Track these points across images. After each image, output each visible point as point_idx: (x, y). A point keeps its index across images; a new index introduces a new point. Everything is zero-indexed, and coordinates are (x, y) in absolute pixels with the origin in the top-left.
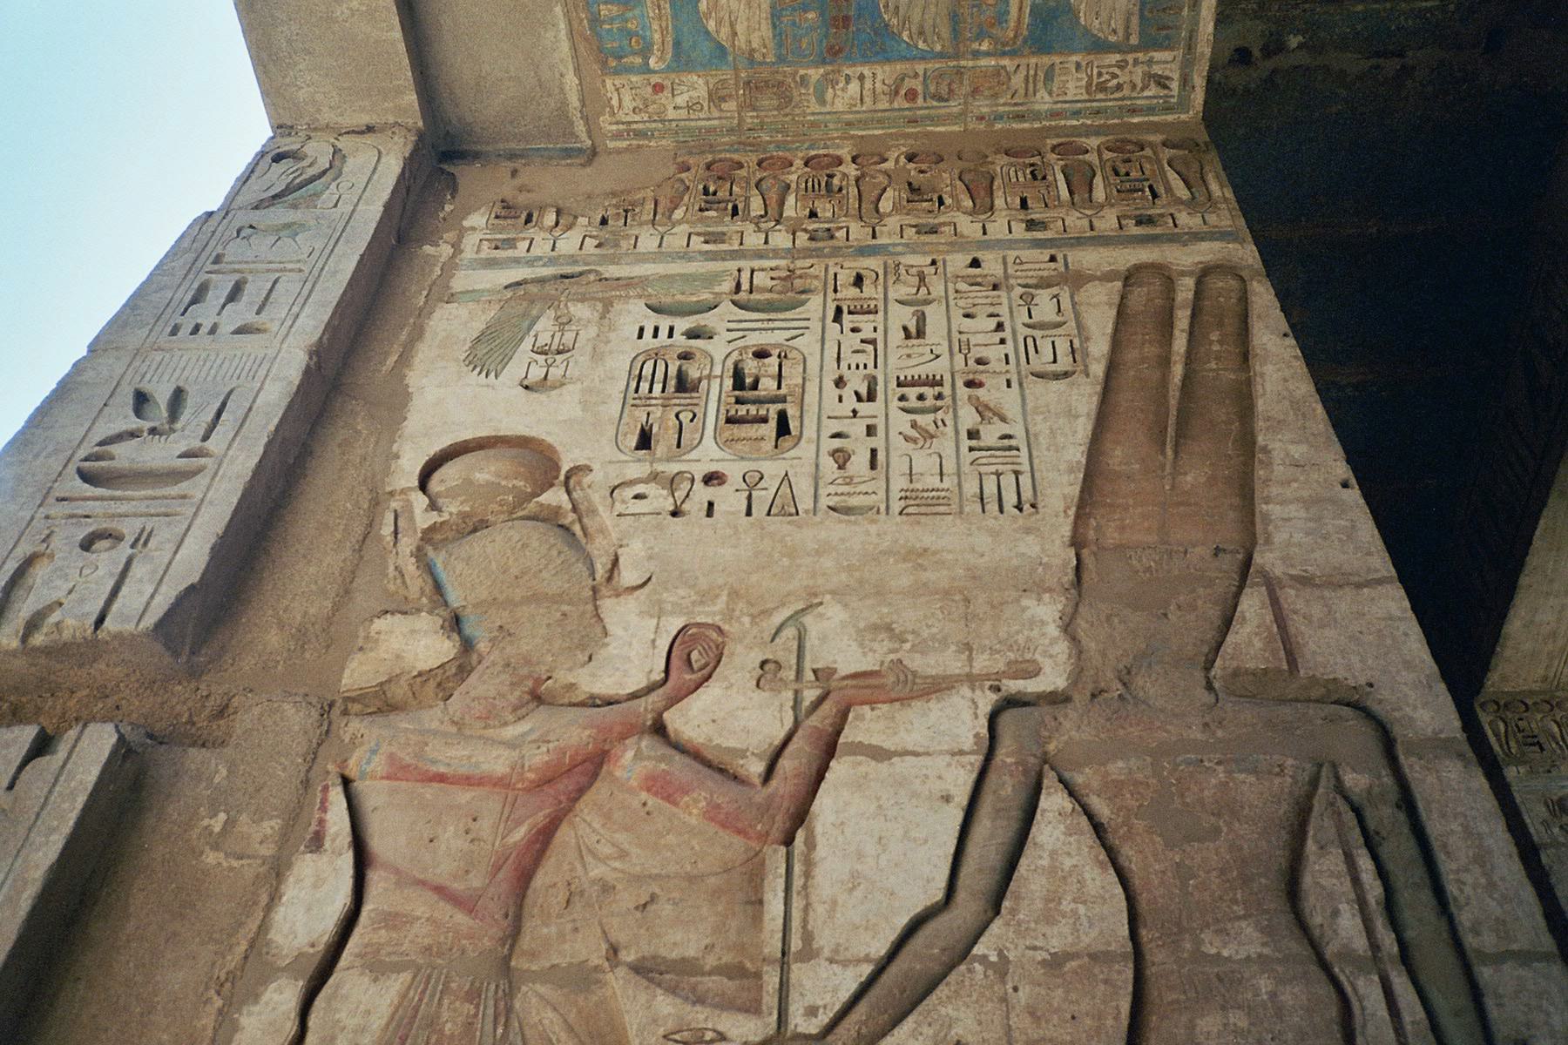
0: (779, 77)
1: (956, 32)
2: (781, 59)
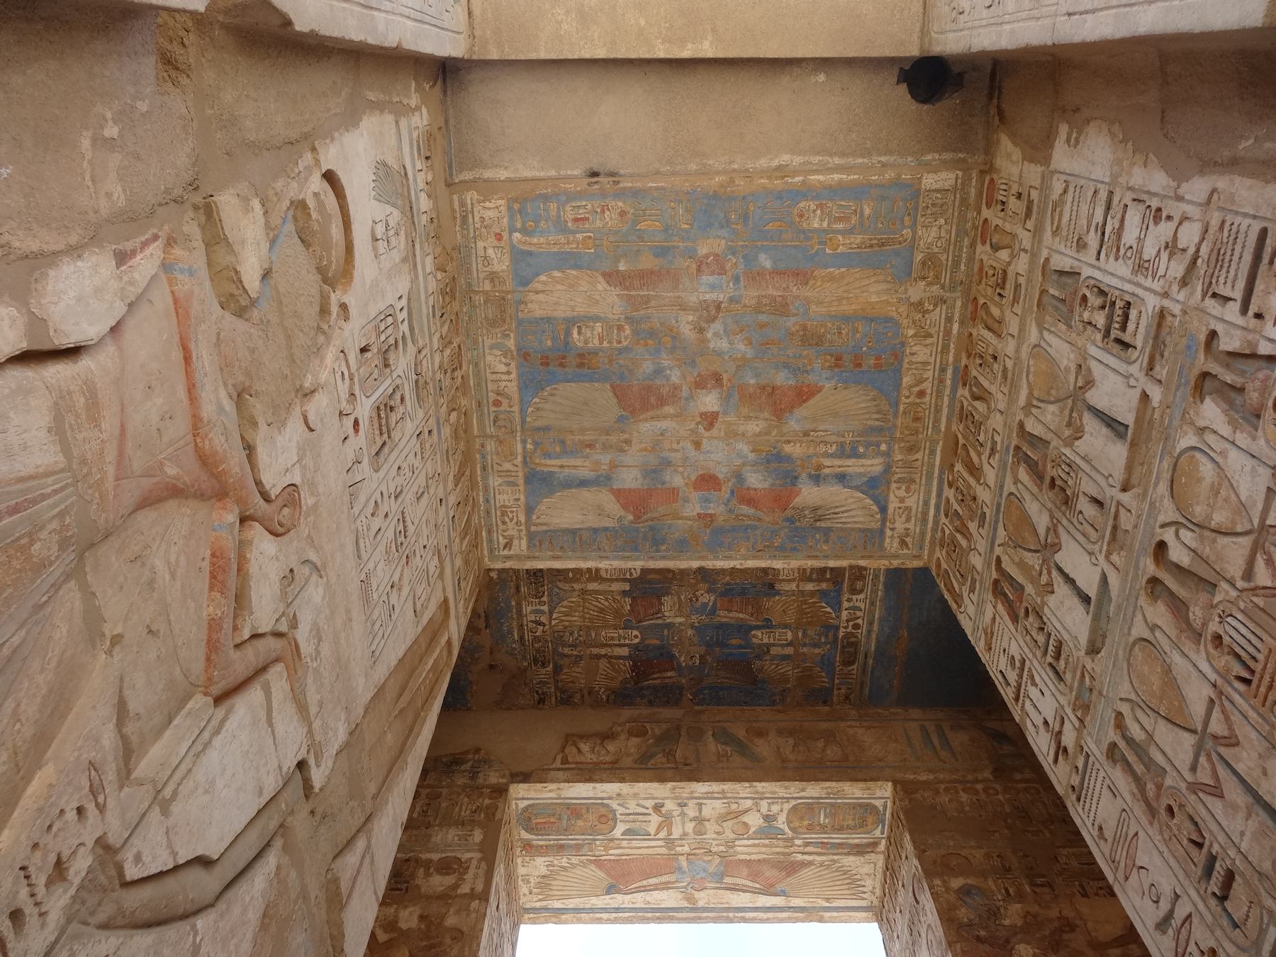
0: (508, 319)
1: (539, 429)
2: (520, 323)
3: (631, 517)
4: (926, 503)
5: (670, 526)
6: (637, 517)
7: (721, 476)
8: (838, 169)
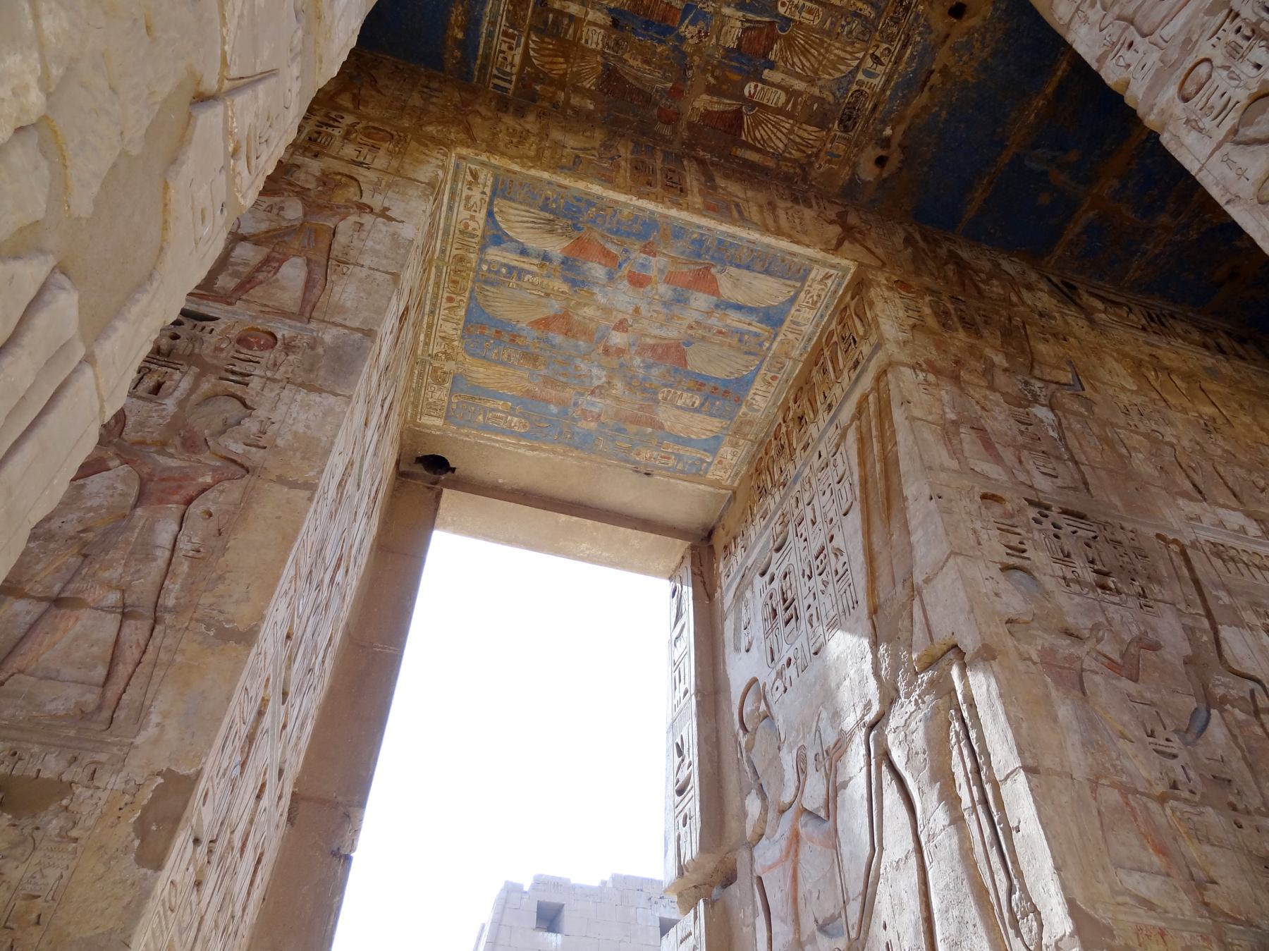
2: (731, 419)
3: (713, 270)
4: (450, 208)
5: (683, 253)
6: (708, 269)
7: (626, 282)
8: (497, 441)
